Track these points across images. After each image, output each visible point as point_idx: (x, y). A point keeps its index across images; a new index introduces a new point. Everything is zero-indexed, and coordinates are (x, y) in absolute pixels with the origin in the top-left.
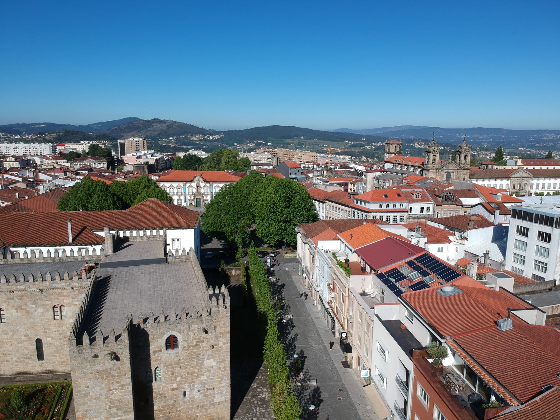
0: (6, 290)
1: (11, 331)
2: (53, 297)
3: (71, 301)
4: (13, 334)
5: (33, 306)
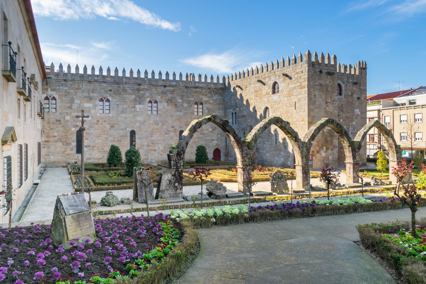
0: (161, 84)
1: (161, 122)
2: (195, 94)
3: (208, 99)
4: (163, 125)
5: (181, 101)
